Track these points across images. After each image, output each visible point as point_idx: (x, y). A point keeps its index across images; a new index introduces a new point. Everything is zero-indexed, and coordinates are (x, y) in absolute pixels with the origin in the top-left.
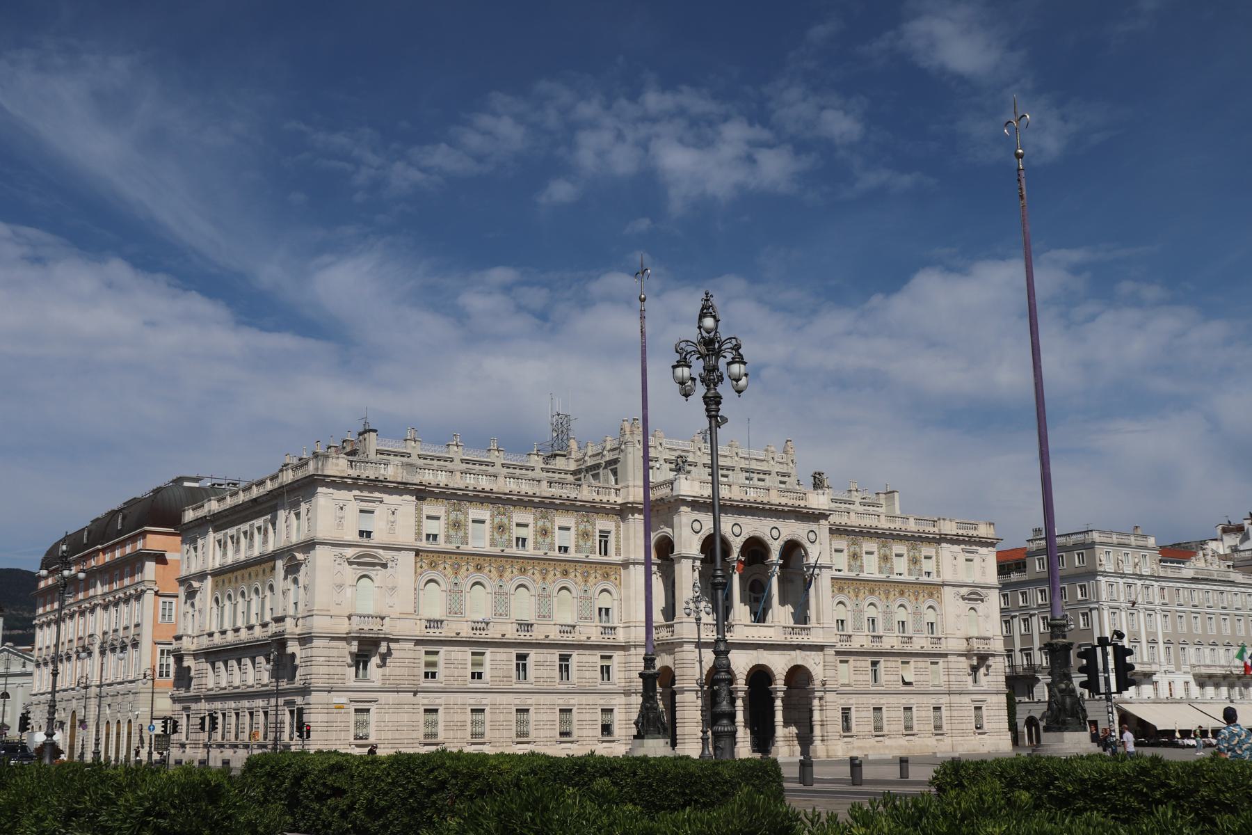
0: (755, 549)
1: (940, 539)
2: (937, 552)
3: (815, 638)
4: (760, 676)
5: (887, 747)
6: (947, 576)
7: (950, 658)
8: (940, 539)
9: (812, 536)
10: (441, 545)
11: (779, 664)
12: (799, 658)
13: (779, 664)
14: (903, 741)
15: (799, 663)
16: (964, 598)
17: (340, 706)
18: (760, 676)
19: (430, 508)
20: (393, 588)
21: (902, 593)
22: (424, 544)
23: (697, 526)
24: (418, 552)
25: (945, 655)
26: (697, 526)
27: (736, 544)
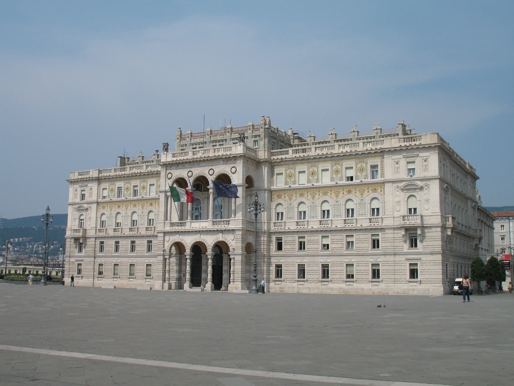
0: (201, 183)
1: (382, 153)
2: (382, 162)
3: (231, 226)
4: (198, 249)
5: (328, 288)
6: (389, 175)
7: (387, 231)
8: (382, 153)
9: (233, 170)
10: (107, 199)
11: (210, 241)
12: (220, 237)
13: (210, 241)
14: (343, 286)
15: (221, 240)
16: (402, 190)
17: (73, 262)
18: (198, 249)
19: (104, 185)
20: (90, 218)
21: (350, 192)
22: (100, 200)
23: (170, 176)
24: (98, 203)
25: (382, 229)
26: (170, 176)
27: (211, 179)
